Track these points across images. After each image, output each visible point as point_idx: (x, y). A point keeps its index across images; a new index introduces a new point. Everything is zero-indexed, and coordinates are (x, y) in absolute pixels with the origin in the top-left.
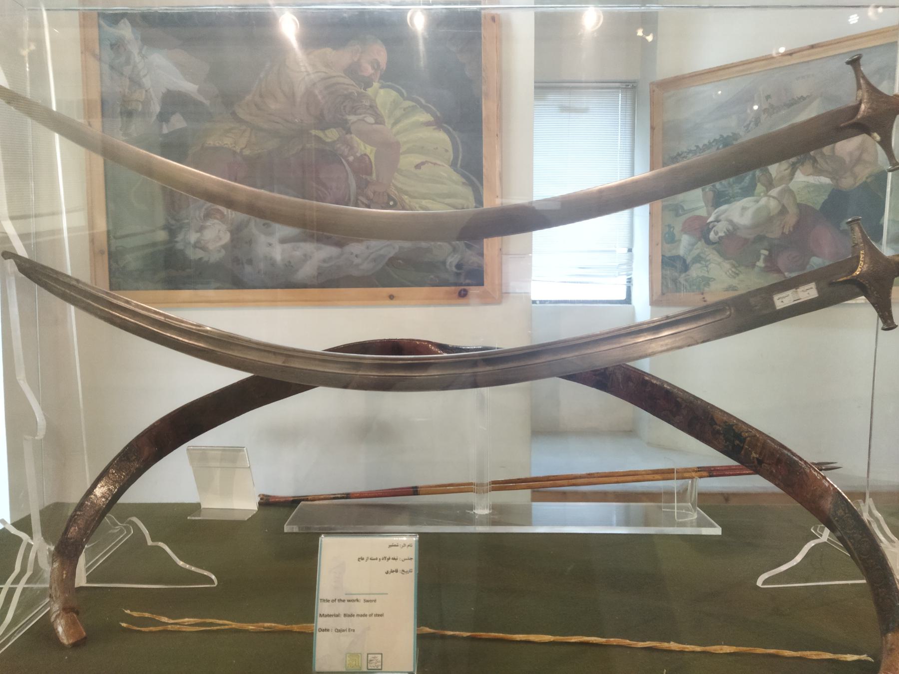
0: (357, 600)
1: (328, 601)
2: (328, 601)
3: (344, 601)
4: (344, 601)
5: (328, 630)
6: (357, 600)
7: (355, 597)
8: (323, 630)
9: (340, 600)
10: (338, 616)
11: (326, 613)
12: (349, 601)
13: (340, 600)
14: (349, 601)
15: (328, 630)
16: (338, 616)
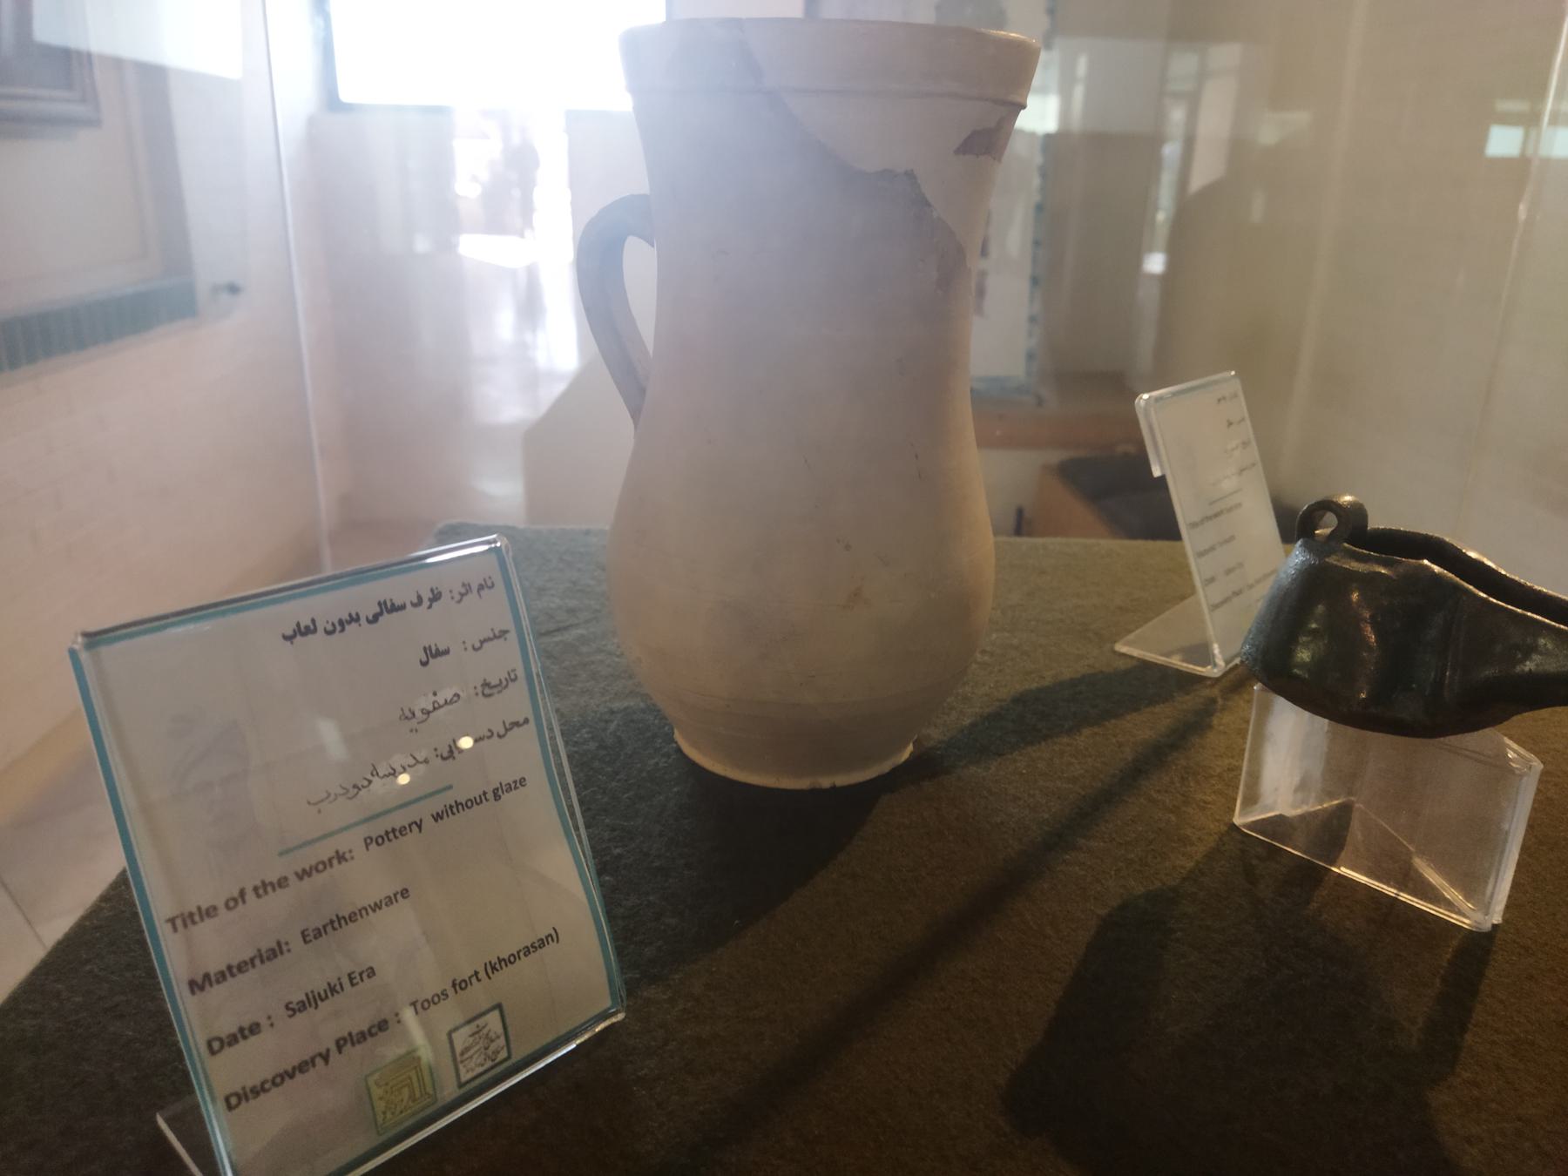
0: (341, 858)
1: (211, 912)
2: (211, 912)
3: (282, 883)
4: (282, 883)
5: (255, 1029)
6: (341, 858)
7: (325, 851)
8: (233, 1040)
9: (262, 889)
10: (276, 952)
11: (213, 967)
12: (303, 875)
13: (262, 889)
14: (303, 875)
15: (255, 1029)
16: (276, 952)
